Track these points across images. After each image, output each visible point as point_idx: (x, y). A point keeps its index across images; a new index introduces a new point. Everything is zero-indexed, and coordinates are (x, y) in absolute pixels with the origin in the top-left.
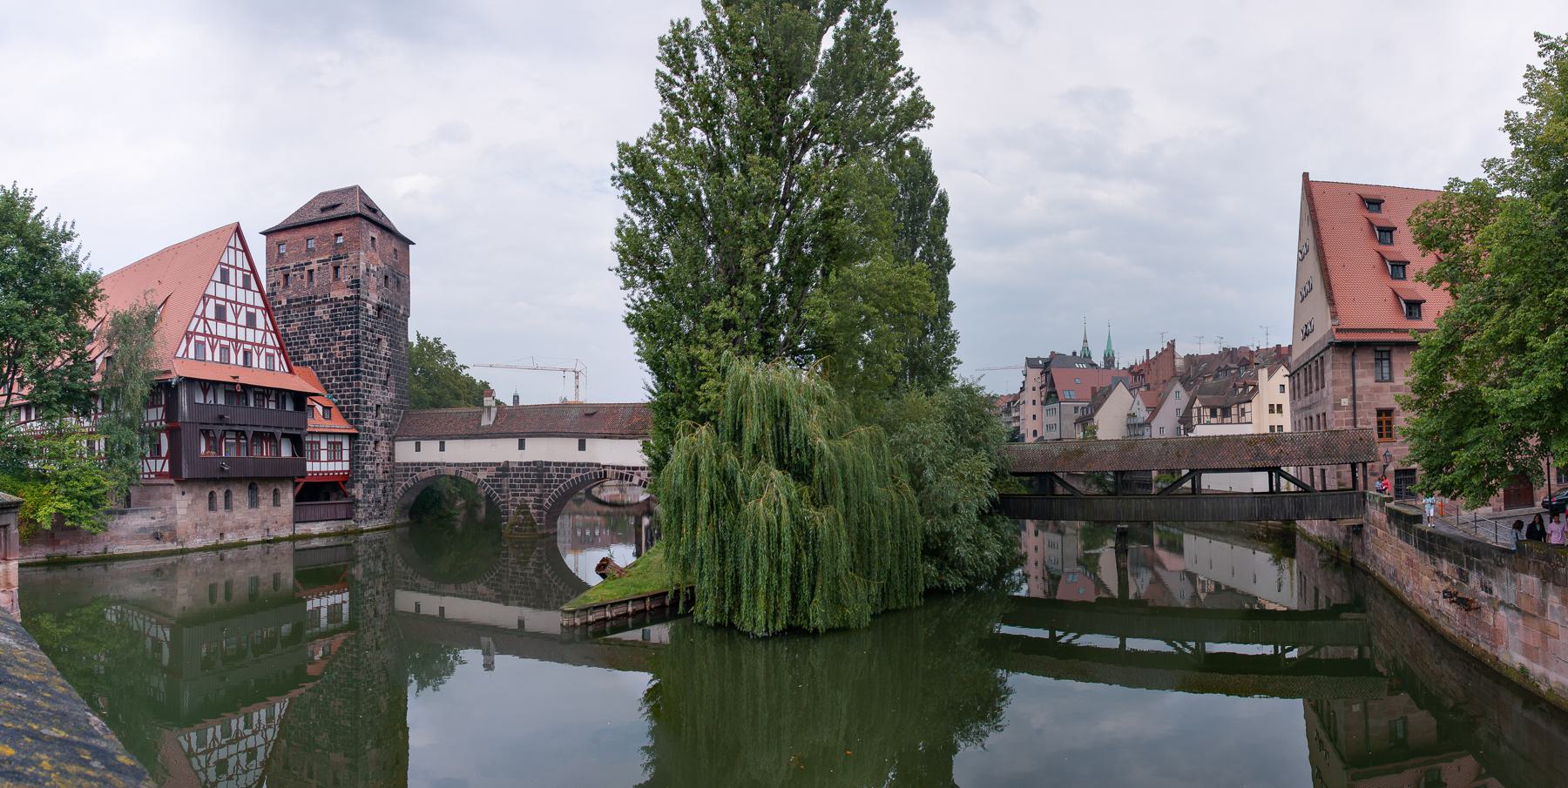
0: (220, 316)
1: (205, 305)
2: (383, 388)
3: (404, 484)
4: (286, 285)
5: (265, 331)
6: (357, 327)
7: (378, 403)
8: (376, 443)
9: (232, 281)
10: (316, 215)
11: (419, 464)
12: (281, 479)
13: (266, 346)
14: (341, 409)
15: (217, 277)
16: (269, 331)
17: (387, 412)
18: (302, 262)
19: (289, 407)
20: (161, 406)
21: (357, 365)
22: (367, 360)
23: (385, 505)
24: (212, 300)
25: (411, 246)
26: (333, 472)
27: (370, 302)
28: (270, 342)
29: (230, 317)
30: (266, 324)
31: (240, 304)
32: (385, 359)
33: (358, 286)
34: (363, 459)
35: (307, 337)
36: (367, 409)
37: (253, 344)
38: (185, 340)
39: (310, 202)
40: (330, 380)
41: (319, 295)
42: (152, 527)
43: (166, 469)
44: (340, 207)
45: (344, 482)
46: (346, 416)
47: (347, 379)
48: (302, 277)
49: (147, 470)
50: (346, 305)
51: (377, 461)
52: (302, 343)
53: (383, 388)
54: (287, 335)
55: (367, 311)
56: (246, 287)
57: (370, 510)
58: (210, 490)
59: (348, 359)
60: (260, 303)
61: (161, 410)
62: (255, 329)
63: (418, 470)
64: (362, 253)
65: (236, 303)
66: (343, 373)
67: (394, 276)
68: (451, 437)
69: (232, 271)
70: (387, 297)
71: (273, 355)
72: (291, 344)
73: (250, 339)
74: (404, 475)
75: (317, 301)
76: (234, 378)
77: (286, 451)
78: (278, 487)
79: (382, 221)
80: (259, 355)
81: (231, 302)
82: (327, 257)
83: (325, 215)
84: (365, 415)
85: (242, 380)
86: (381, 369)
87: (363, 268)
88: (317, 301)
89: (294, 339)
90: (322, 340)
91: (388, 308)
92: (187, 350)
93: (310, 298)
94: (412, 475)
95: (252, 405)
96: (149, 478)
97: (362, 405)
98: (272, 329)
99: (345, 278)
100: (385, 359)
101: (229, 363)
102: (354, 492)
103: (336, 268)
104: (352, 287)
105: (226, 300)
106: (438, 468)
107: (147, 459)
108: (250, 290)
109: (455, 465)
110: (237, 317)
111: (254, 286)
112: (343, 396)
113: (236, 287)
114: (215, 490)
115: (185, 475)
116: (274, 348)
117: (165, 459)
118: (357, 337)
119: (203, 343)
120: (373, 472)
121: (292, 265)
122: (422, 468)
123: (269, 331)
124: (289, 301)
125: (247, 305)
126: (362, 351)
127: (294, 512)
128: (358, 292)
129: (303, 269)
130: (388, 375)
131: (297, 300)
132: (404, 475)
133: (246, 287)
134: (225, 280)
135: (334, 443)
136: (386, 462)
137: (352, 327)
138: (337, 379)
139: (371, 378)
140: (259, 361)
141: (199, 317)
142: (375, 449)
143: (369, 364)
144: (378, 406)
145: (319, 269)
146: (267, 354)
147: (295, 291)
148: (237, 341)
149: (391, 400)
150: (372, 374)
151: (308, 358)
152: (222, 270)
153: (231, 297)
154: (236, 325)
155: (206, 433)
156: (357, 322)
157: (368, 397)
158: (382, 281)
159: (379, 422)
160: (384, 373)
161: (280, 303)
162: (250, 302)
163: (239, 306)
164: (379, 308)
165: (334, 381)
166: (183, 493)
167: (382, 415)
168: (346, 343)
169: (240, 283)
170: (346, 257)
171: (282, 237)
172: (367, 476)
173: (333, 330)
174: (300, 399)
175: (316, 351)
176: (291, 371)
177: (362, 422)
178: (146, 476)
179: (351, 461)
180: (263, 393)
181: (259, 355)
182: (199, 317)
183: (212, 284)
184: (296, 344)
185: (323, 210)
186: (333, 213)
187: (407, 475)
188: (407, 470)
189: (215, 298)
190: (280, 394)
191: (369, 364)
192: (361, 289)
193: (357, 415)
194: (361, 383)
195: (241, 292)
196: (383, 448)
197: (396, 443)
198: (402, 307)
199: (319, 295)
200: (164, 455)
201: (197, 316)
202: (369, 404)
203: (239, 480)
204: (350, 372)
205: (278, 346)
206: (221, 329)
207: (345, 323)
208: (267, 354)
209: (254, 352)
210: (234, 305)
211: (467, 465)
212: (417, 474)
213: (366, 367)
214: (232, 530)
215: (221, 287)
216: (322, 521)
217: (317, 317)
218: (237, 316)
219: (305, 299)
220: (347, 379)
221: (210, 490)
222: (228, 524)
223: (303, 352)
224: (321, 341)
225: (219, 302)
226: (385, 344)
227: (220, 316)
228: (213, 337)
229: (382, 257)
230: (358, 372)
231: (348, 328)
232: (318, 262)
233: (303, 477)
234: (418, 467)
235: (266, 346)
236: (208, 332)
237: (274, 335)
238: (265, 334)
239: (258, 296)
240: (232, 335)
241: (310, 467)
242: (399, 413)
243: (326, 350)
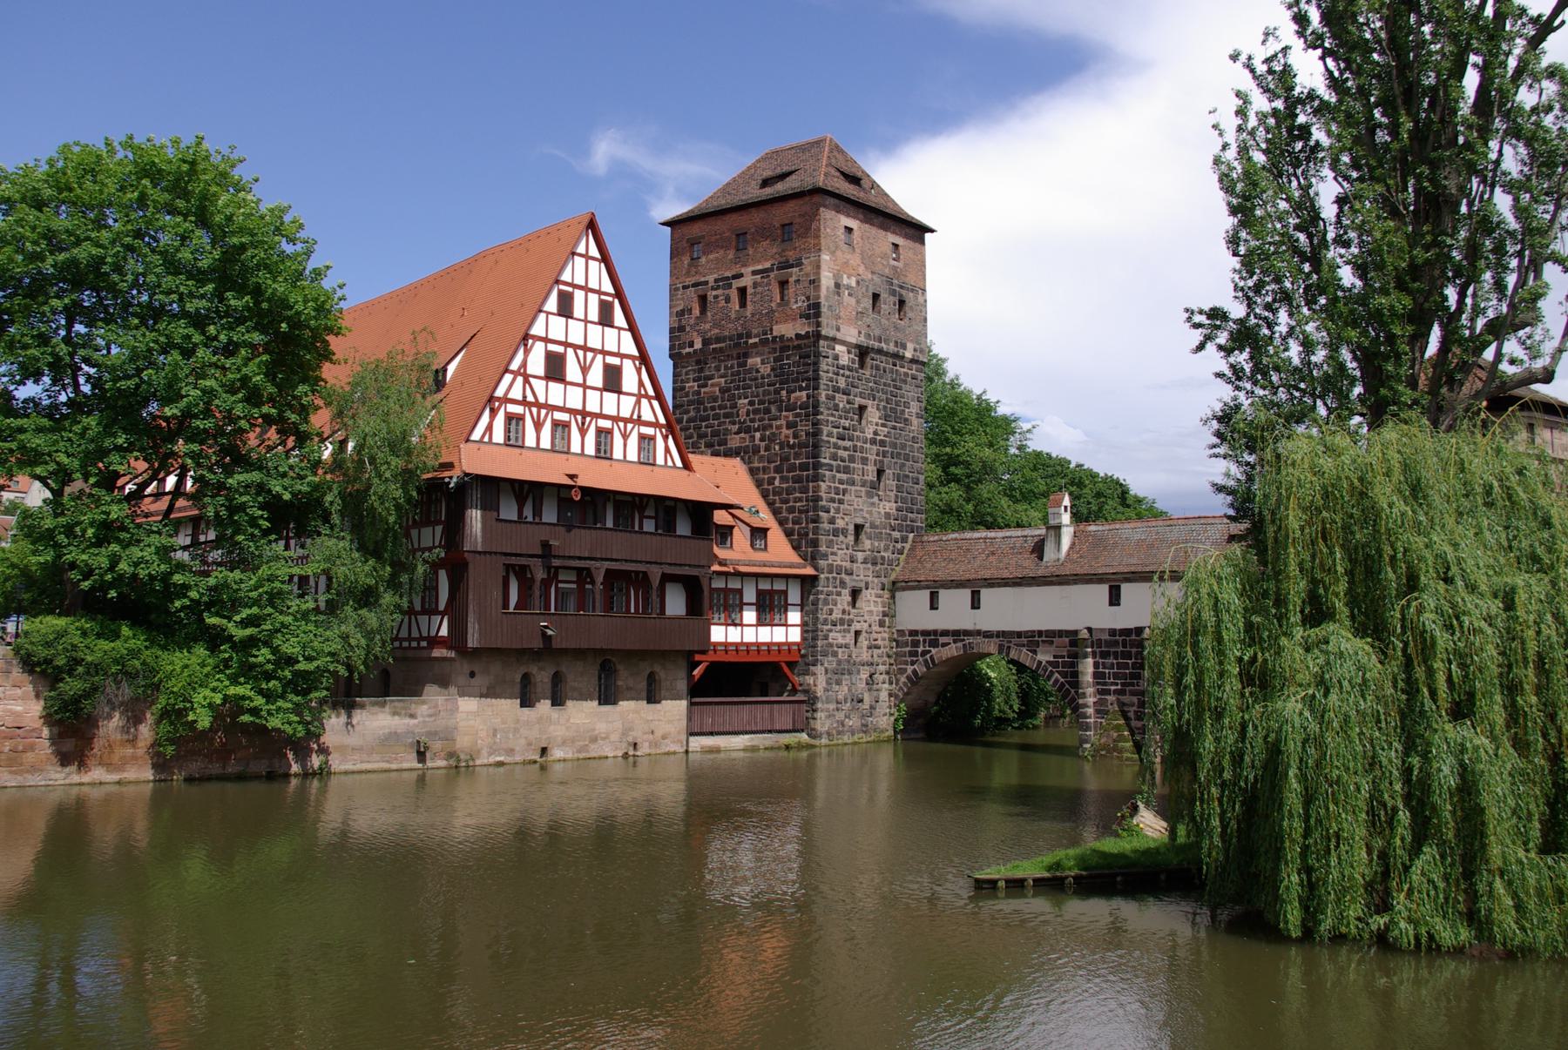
0: (555, 369)
1: (527, 352)
2: (870, 495)
3: (910, 669)
4: (703, 310)
5: (639, 397)
6: (816, 388)
7: (859, 521)
8: (855, 593)
9: (578, 311)
10: (755, 193)
11: (935, 632)
12: (664, 656)
13: (639, 422)
14: (788, 534)
15: (552, 304)
16: (647, 396)
17: (879, 537)
18: (728, 274)
19: (683, 528)
20: (438, 522)
21: (816, 456)
22: (836, 446)
23: (872, 707)
24: (539, 347)
25: (928, 236)
26: (769, 645)
27: (843, 343)
28: (647, 415)
29: (573, 371)
30: (641, 384)
31: (591, 350)
32: (873, 442)
33: (818, 315)
34: (825, 622)
35: (734, 406)
36: (836, 533)
37: (616, 419)
38: (487, 412)
39: (749, 168)
40: (771, 481)
41: (755, 331)
42: (410, 732)
43: (444, 632)
44: (793, 177)
45: (791, 665)
46: (796, 548)
47: (797, 480)
48: (728, 300)
49: (415, 634)
50: (798, 347)
51: (856, 626)
52: (726, 416)
53: (870, 495)
54: (700, 402)
55: (836, 358)
56: (606, 320)
57: (840, 716)
58: (523, 670)
59: (801, 446)
60: (629, 347)
61: (439, 529)
62: (620, 392)
63: (934, 644)
64: (825, 257)
65: (585, 348)
66: (792, 468)
67: (893, 293)
68: (991, 583)
69: (579, 296)
70: (877, 332)
71: (652, 438)
72: (706, 419)
73: (610, 409)
75: (751, 341)
76: (572, 477)
77: (675, 604)
78: (657, 668)
79: (872, 199)
80: (625, 436)
81: (575, 347)
82: (768, 265)
83: (769, 192)
84: (830, 544)
85: (583, 481)
86: (864, 461)
87: (827, 280)
88: (751, 341)
89: (713, 408)
90: (756, 412)
91: (880, 351)
92: (489, 428)
93: (740, 336)
94: (924, 653)
95: (610, 524)
96: (419, 648)
97: (826, 526)
98: (651, 392)
99: (798, 304)
100: (873, 442)
101: (568, 452)
102: (810, 680)
103: (783, 284)
104: (808, 317)
105: (566, 344)
107: (416, 614)
108: (612, 326)
110: (585, 370)
111: (619, 318)
112: (791, 510)
113: (586, 321)
114: (534, 669)
115: (473, 641)
116: (656, 425)
117: (443, 614)
118: (816, 406)
119: (520, 418)
120: (847, 646)
121: (711, 278)
122: (942, 640)
123: (647, 396)
124: (706, 342)
125: (604, 353)
126: (825, 430)
127: (690, 719)
128: (818, 324)
129: (730, 286)
130: (880, 472)
131: (718, 340)
133: (606, 320)
134: (565, 310)
135: (771, 592)
136: (876, 628)
137: (807, 388)
138: (783, 479)
139: (844, 477)
140: (626, 448)
141: (516, 374)
142: (854, 603)
143: (841, 453)
144: (858, 528)
145: (755, 285)
146: (642, 437)
147: (716, 325)
148: (584, 413)
149: (888, 515)
150: (847, 470)
151: (735, 441)
152: (561, 294)
153: (576, 337)
154: (584, 386)
155: (522, 573)
156: (817, 378)
157: (838, 511)
158: (868, 302)
159: (860, 556)
160: (871, 469)
161: (691, 345)
162: (611, 346)
163: (590, 355)
164: (863, 353)
165: (777, 483)
166: (472, 675)
167: (867, 544)
168: (797, 415)
169: (594, 315)
170: (799, 264)
171: (696, 230)
172: (835, 654)
173: (777, 392)
174: (700, 513)
175: (748, 430)
176: (687, 466)
177: (825, 556)
178: (405, 644)
179: (804, 625)
180: (630, 506)
181: (625, 436)
182: (516, 374)
183: (542, 316)
184: (716, 417)
185: (766, 183)
186: (781, 188)
188: (915, 644)
189: (546, 340)
190: (666, 509)
191: (841, 453)
192: (823, 320)
193: (815, 543)
194: (823, 486)
195: (595, 332)
196: (872, 604)
197: (898, 594)
198: (910, 346)
199: (755, 331)
200: (442, 607)
201: (512, 372)
202: (840, 523)
203: (579, 654)
204: (804, 467)
205: (662, 420)
206: (555, 393)
207: (796, 380)
208: (642, 437)
209: (617, 434)
210: (580, 353)
211: (1019, 634)
212: (934, 651)
213: (834, 457)
214: (564, 743)
215: (557, 324)
216: (747, 733)
217: (751, 369)
218: (585, 370)
219: (731, 339)
220: (797, 480)
221: (523, 670)
222: (558, 731)
223: (727, 432)
224: (756, 412)
225: (552, 347)
226: (873, 415)
227: (555, 369)
228: (539, 406)
229: (867, 260)
230: (817, 466)
231: (801, 389)
232: (754, 273)
233: (703, 652)
234: (933, 637)
235: (639, 422)
236: (530, 398)
237: (656, 404)
238: (638, 403)
239: (627, 337)
240: (574, 401)
241: (718, 634)
242: (904, 540)
243: (765, 428)
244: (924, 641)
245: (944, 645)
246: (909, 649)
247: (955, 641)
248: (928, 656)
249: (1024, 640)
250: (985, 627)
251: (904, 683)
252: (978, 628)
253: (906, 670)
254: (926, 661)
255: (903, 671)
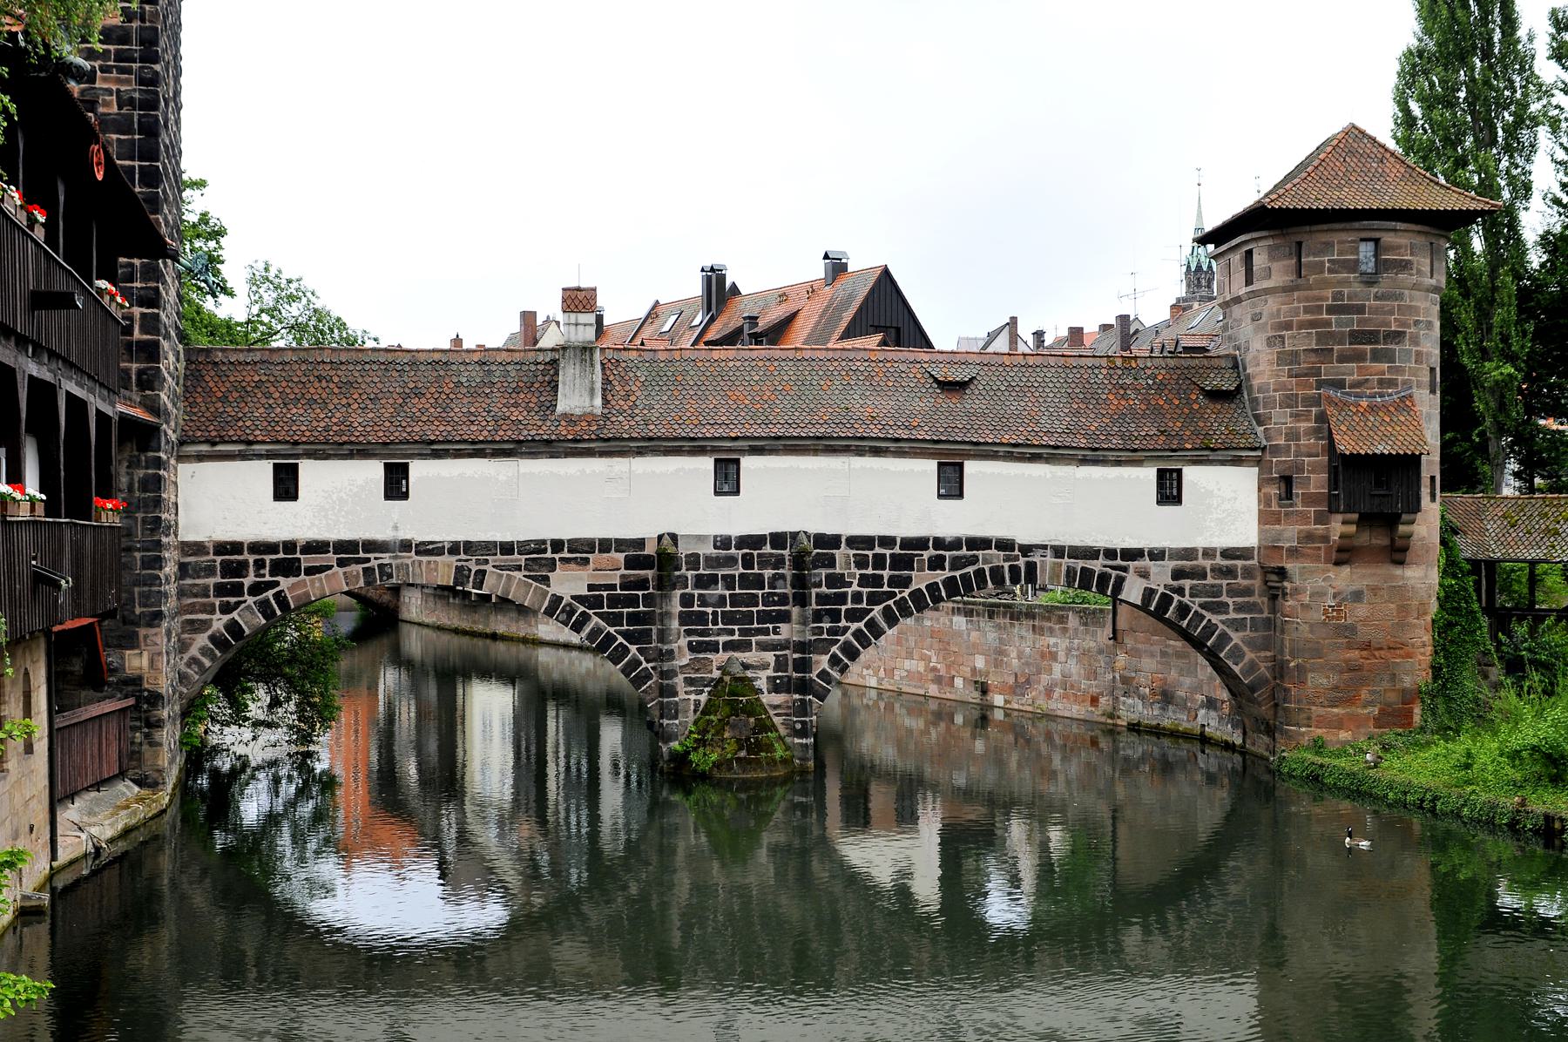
3: (219, 622)
11: (290, 546)
63: (288, 568)
68: (437, 450)
74: (220, 590)
94: (256, 589)
102: (136, 662)
106: (375, 560)
109: (454, 548)
122: (306, 561)
132: (220, 590)
187: (237, 590)
188: (239, 569)
211: (507, 548)
212: (285, 583)
244: (260, 565)
245: (311, 571)
246: (211, 581)
247: (341, 563)
248: (270, 594)
249: (521, 559)
250: (418, 535)
251: (204, 651)
252: (405, 534)
253: (206, 625)
254: (264, 607)
255: (196, 627)
